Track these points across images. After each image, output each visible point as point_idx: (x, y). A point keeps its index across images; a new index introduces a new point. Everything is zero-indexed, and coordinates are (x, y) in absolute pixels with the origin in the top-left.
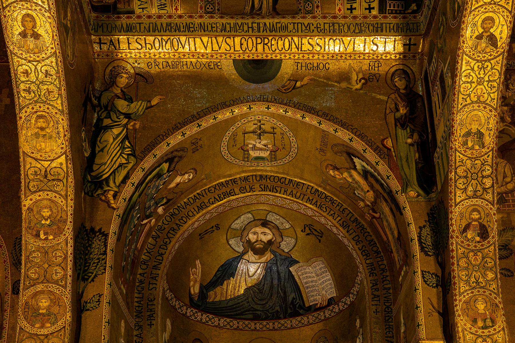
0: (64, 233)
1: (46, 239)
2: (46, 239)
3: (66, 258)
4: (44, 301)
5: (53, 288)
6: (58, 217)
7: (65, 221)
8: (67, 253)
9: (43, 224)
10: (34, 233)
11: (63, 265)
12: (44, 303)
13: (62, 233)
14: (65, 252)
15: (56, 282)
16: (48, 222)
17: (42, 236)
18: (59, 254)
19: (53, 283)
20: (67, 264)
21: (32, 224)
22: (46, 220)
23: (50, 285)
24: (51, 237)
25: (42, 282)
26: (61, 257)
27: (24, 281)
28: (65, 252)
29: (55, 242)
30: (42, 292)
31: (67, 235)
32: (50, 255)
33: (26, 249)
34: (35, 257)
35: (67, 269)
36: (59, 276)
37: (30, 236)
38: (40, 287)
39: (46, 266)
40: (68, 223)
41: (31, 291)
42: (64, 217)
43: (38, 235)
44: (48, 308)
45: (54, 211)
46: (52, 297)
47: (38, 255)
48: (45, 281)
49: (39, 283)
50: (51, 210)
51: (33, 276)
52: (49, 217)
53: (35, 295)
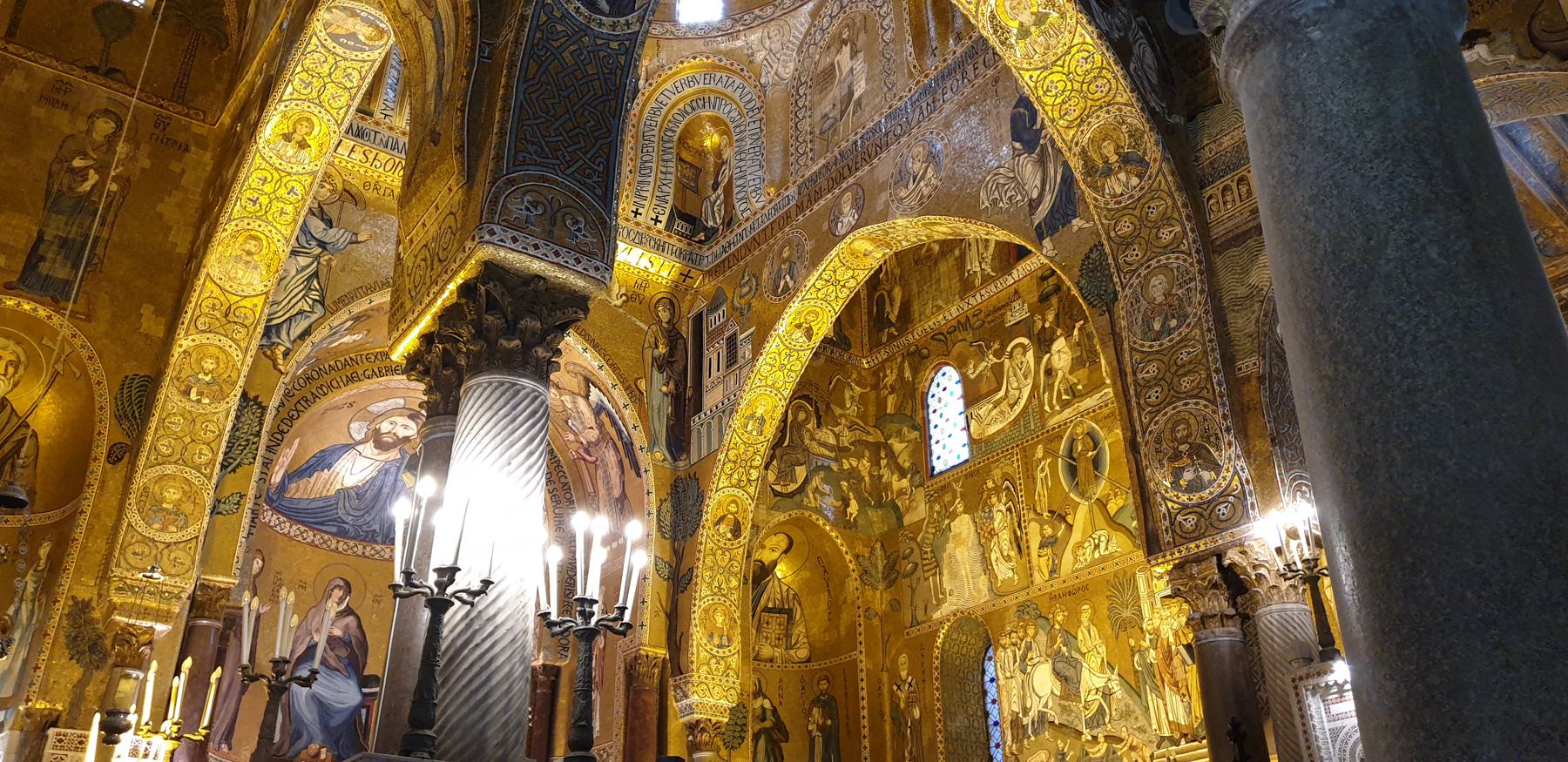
0: (228, 399)
1: (199, 401)
2: (199, 401)
3: (220, 435)
4: (172, 490)
5: (192, 475)
6: (225, 376)
7: (234, 384)
8: (224, 430)
9: (199, 380)
10: (183, 388)
11: (213, 445)
12: (172, 495)
13: (224, 399)
14: (221, 427)
15: (197, 468)
16: (208, 378)
17: (193, 396)
18: (211, 427)
19: (192, 468)
20: (220, 444)
21: (183, 375)
22: (207, 374)
23: (188, 469)
24: (206, 401)
25: (176, 463)
26: (214, 432)
27: (149, 454)
28: (221, 427)
29: (210, 409)
30: (172, 477)
31: (231, 403)
32: (198, 426)
33: (163, 407)
34: (174, 423)
35: (217, 453)
36: (204, 459)
37: (175, 391)
38: (170, 469)
39: (187, 440)
40: (238, 387)
41: (157, 471)
42: (234, 375)
43: (187, 393)
44: (178, 504)
45: (222, 365)
46: (187, 488)
47: (179, 420)
48: (180, 462)
49: (170, 463)
50: (218, 363)
51: (164, 449)
52: (211, 372)
53: (162, 478)
